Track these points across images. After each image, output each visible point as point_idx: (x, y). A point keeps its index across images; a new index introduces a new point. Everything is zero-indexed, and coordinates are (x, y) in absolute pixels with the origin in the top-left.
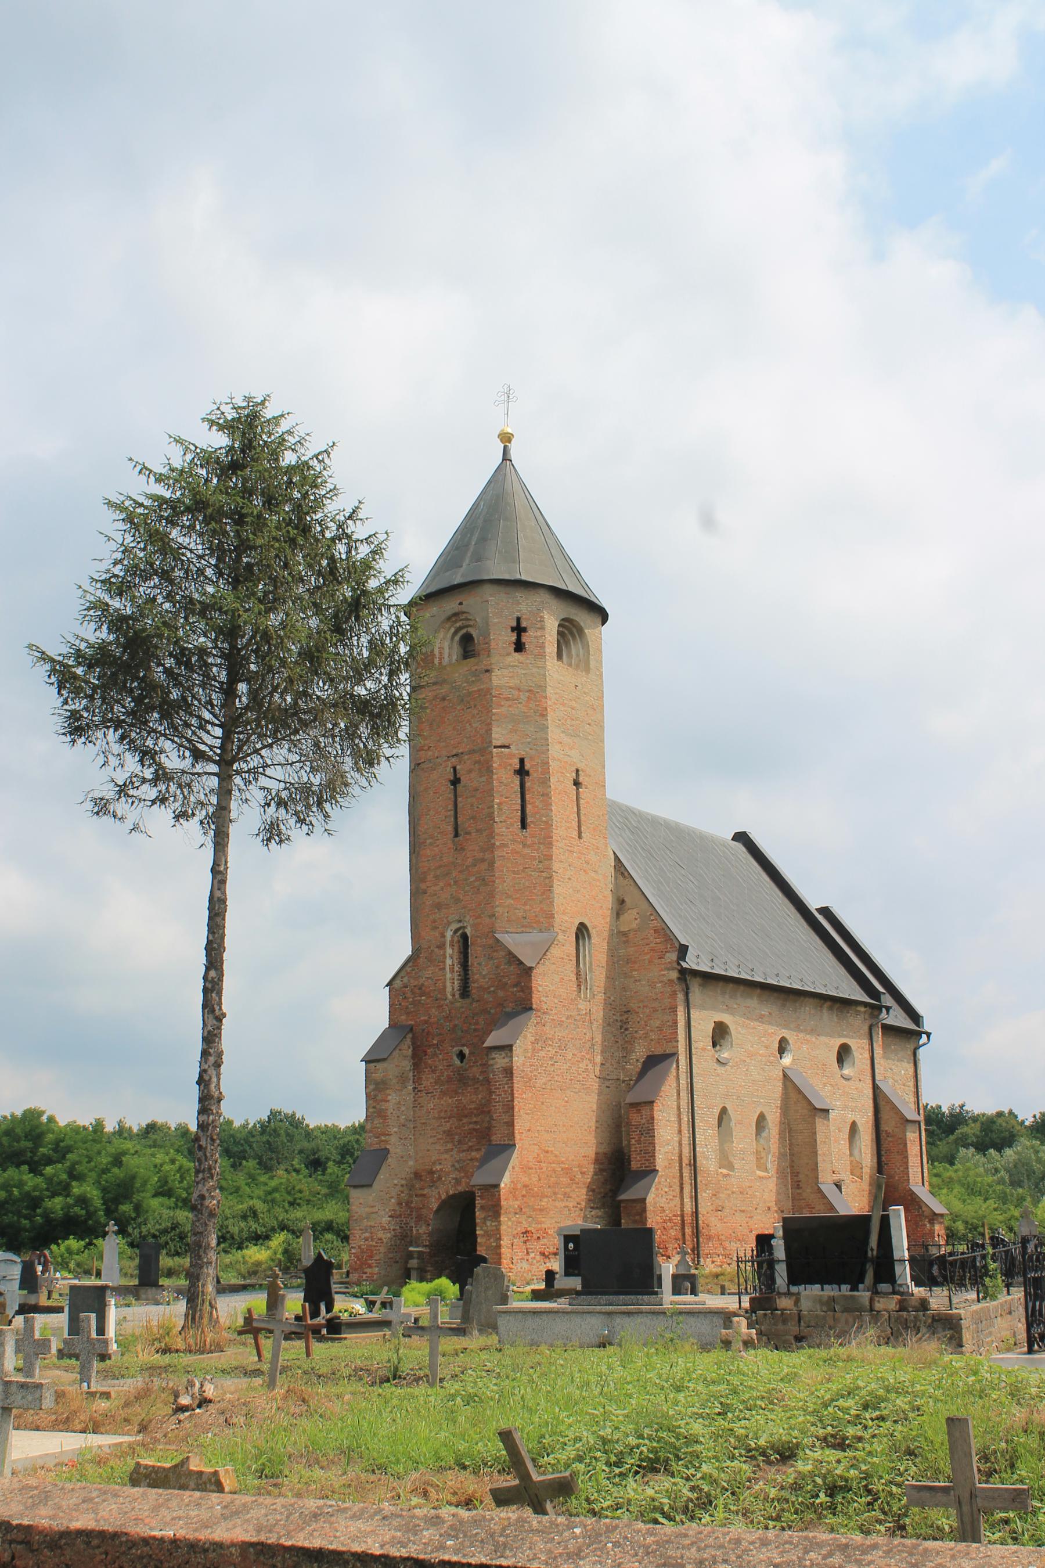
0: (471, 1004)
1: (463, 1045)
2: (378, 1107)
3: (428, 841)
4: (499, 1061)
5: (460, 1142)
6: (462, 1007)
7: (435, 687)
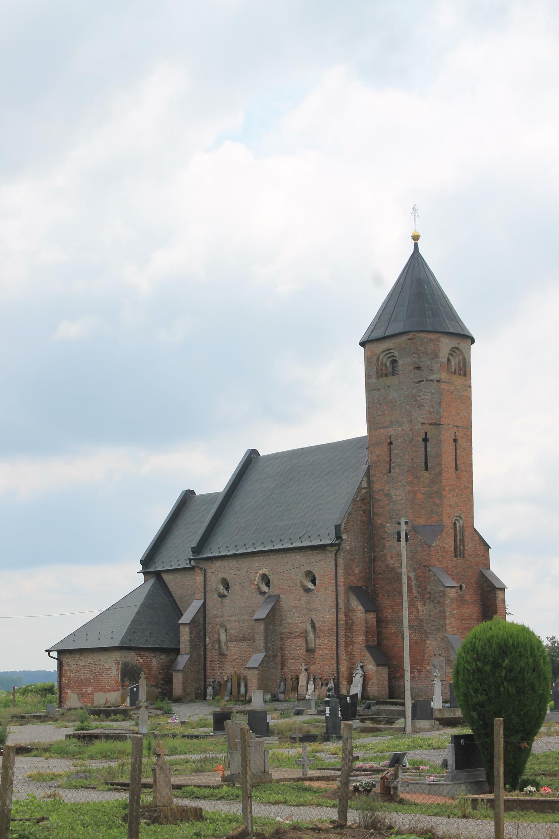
0: (465, 562)
1: (463, 583)
2: (452, 611)
3: (446, 469)
4: (500, 595)
5: (461, 633)
6: (461, 563)
7: (448, 385)
